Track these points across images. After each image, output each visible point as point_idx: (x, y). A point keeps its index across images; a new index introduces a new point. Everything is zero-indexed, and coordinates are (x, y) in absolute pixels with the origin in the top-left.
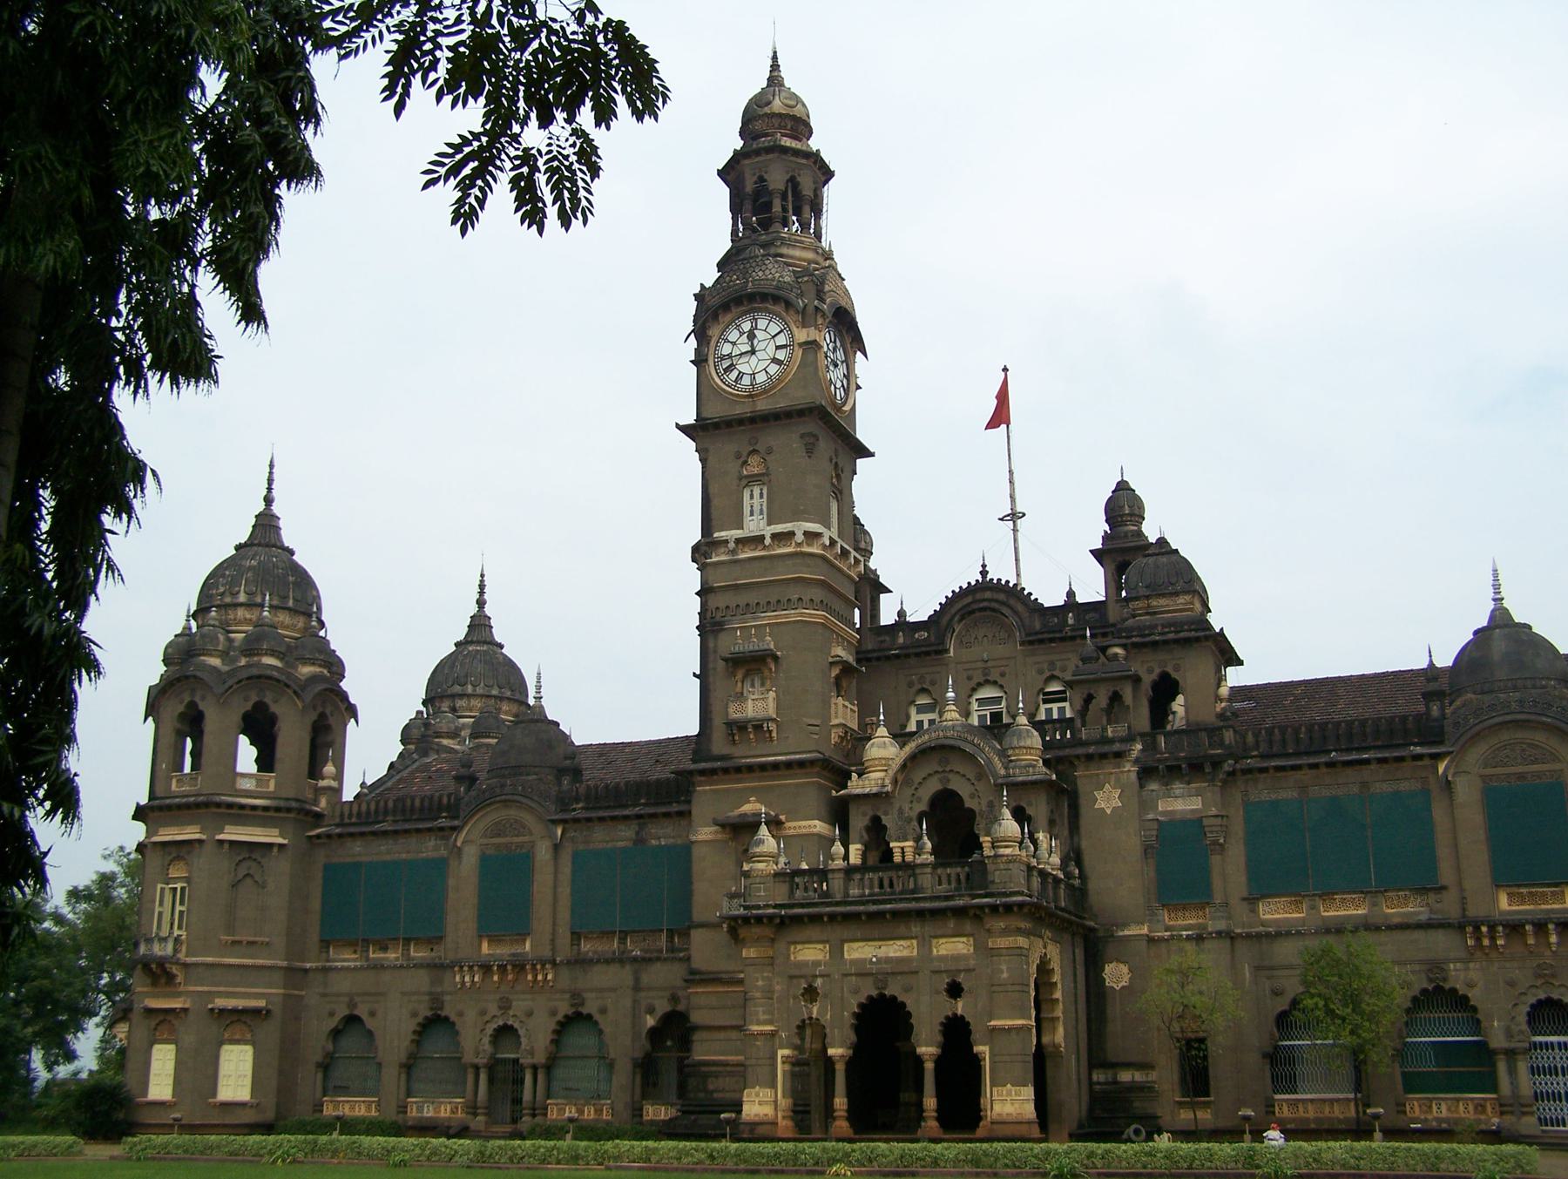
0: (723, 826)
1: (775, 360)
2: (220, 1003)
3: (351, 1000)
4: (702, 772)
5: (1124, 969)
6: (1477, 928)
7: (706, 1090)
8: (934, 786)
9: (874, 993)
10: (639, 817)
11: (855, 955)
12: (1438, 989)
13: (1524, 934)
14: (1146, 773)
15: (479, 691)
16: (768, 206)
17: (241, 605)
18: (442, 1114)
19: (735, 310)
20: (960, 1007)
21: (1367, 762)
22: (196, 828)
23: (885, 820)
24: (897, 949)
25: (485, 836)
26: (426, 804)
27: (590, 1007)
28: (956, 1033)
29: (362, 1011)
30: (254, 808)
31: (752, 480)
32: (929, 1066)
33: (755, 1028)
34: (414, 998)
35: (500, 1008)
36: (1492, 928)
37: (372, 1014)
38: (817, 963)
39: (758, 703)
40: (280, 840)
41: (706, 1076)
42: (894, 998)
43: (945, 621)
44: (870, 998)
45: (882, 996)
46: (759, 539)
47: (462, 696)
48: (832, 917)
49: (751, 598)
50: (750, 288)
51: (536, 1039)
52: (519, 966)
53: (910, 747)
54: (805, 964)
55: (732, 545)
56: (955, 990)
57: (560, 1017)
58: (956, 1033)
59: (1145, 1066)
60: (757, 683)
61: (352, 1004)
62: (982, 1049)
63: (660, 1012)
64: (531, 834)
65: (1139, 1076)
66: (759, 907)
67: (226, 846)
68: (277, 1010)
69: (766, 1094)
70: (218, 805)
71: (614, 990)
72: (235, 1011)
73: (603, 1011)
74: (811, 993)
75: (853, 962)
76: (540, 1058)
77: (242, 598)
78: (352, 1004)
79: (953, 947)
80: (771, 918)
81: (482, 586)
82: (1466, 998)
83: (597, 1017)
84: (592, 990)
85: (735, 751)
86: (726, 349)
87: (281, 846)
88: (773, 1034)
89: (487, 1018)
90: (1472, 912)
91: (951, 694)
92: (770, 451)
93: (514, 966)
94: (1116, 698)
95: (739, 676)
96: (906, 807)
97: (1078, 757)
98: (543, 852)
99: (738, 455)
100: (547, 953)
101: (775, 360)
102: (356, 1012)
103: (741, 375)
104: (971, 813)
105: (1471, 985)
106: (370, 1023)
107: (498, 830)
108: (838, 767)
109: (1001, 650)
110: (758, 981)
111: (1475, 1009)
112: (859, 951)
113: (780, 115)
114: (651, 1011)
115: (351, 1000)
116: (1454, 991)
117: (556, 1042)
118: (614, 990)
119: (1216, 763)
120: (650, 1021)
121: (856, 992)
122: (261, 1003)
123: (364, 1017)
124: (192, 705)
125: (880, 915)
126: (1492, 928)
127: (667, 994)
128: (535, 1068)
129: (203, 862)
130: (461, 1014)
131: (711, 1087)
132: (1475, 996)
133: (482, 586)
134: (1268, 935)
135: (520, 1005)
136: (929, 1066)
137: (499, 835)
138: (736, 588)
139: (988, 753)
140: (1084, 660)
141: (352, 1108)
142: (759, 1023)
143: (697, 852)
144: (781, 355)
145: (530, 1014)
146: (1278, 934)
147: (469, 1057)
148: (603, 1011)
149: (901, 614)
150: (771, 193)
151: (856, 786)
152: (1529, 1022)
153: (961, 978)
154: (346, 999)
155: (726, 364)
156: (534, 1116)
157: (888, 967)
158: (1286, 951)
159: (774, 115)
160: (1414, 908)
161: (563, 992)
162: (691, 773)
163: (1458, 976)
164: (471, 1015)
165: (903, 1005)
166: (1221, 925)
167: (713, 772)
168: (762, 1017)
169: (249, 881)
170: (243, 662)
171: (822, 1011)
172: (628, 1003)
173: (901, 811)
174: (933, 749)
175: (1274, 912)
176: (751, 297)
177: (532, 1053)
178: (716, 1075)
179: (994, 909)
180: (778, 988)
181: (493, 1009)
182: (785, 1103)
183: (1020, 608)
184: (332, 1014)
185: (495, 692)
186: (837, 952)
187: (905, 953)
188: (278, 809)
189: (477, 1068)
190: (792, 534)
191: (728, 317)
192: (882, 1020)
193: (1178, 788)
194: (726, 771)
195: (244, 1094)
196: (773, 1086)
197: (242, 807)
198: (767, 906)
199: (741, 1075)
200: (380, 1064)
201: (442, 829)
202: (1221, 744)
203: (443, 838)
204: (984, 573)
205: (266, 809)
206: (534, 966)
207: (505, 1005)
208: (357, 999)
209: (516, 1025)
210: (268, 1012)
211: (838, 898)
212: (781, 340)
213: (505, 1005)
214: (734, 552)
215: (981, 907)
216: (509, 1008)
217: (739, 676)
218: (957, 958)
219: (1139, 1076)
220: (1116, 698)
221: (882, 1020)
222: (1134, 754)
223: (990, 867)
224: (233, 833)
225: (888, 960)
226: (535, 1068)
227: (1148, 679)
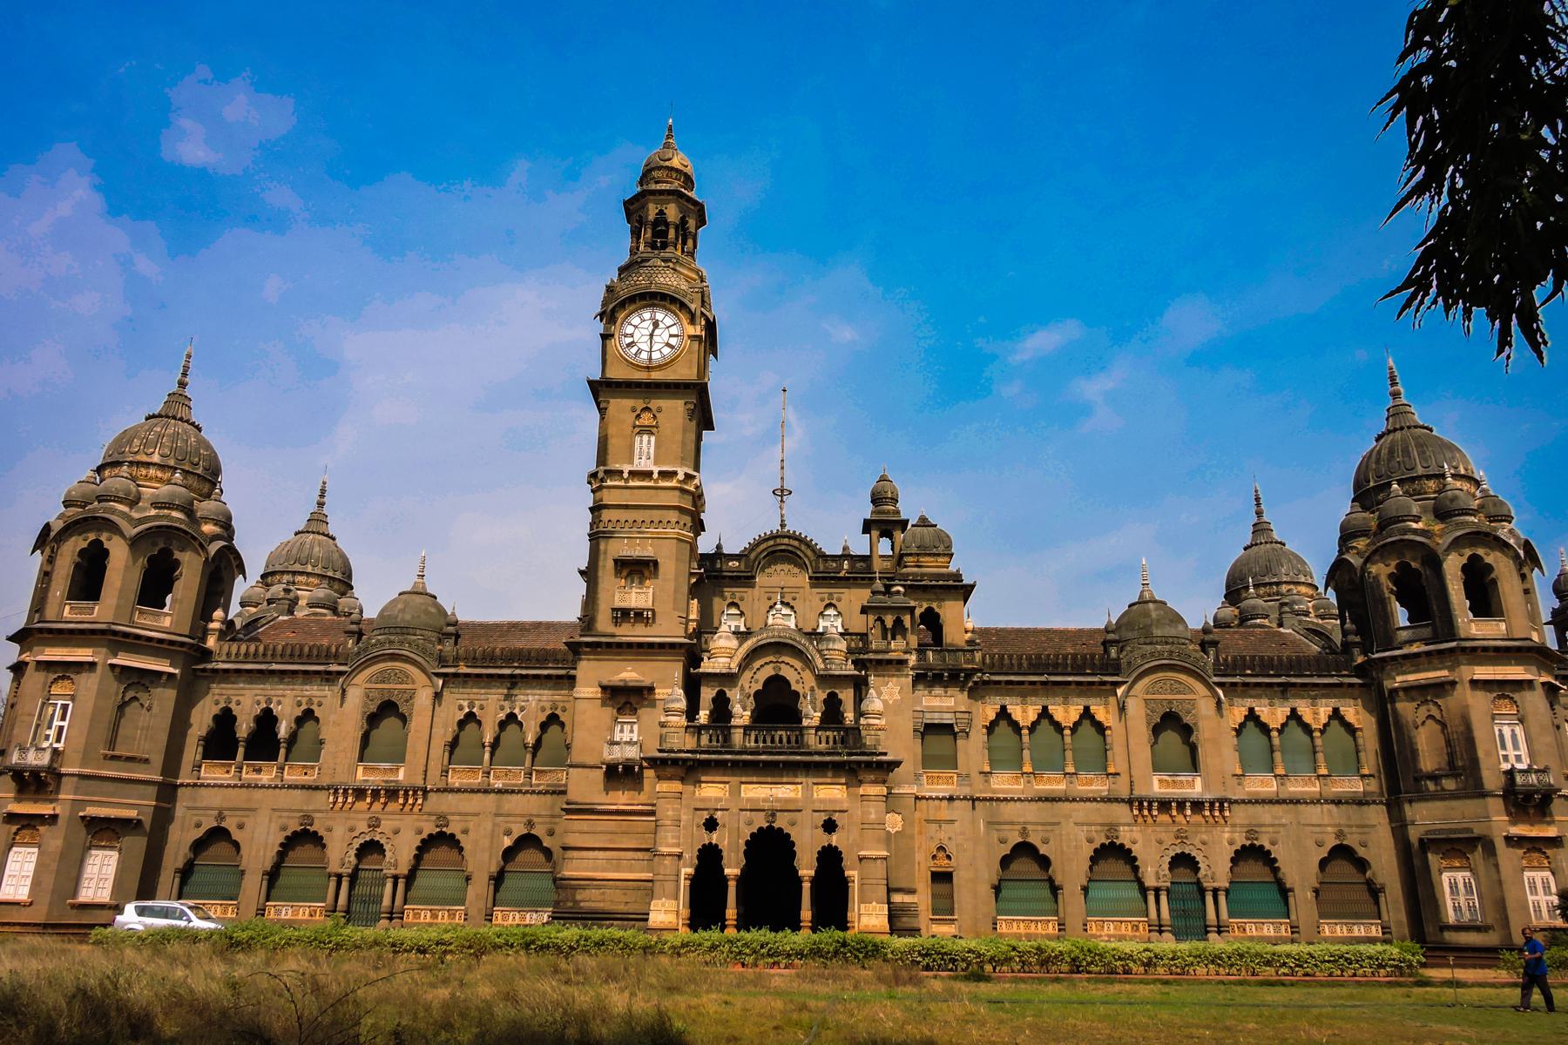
0: (604, 688)
1: (668, 345)
2: (92, 811)
3: (220, 814)
4: (588, 644)
5: (899, 818)
6: (1141, 803)
7: (576, 902)
8: (769, 671)
9: (765, 825)
10: (512, 676)
11: (751, 795)
12: (1112, 843)
13: (1170, 808)
14: (919, 679)
15: (317, 571)
16: (665, 234)
17: (154, 464)
19: (639, 304)
20: (835, 839)
21: (1069, 683)
22: (89, 651)
23: (729, 694)
24: (785, 792)
25: (370, 681)
26: (315, 652)
27: (453, 828)
28: (830, 859)
29: (230, 824)
30: (150, 639)
31: (648, 430)
32: (806, 886)
33: (665, 850)
36: (1150, 803)
37: (241, 827)
38: (720, 800)
39: (637, 597)
40: (171, 670)
41: (575, 888)
42: (780, 830)
43: (752, 556)
44: (761, 829)
45: (770, 828)
46: (649, 475)
47: (301, 573)
48: (735, 764)
49: (639, 515)
50: (653, 290)
51: (400, 853)
52: (392, 793)
53: (750, 643)
54: (709, 799)
55: (626, 475)
56: (830, 826)
57: (424, 835)
58: (830, 859)
59: (912, 892)
60: (636, 581)
61: (221, 817)
62: (852, 873)
63: (516, 835)
65: (907, 899)
66: (671, 751)
67: (117, 670)
68: (147, 821)
69: (670, 904)
70: (115, 633)
71: (477, 815)
72: (107, 820)
74: (711, 825)
75: (748, 800)
76: (404, 869)
77: (156, 458)
78: (221, 817)
79: (832, 793)
80: (685, 760)
81: (323, 491)
82: (1130, 851)
83: (459, 836)
85: (618, 631)
86: (629, 330)
87: (171, 675)
88: (680, 856)
90: (1136, 793)
92: (659, 410)
93: (387, 791)
94: (898, 623)
95: (625, 573)
96: (747, 686)
97: (870, 661)
98: (424, 697)
99: (634, 410)
100: (420, 783)
101: (668, 345)
103: (640, 351)
104: (797, 694)
105: (1134, 843)
106: (236, 835)
107: (383, 677)
108: (692, 654)
109: (792, 581)
110: (667, 811)
111: (1135, 859)
112: (758, 792)
113: (677, 170)
114: (508, 833)
116: (1122, 845)
117: (418, 858)
118: (477, 815)
119: (970, 674)
120: (508, 842)
121: (750, 823)
122: (132, 814)
125: (775, 764)
126: (1150, 803)
128: (396, 878)
129: (88, 684)
130: (330, 830)
131: (578, 897)
132: (1137, 850)
133: (323, 491)
134: (998, 799)
135: (387, 825)
136: (806, 886)
138: (627, 507)
139: (810, 649)
140: (873, 593)
142: (668, 845)
144: (673, 341)
145: (396, 832)
146: (1005, 799)
147: (334, 867)
148: (465, 832)
149: (719, 547)
150: (667, 224)
151: (707, 666)
152: (1170, 869)
153: (836, 817)
155: (629, 340)
156: (391, 919)
157: (778, 806)
158: (1008, 810)
159: (672, 169)
160: (1100, 787)
161: (430, 814)
162: (580, 644)
163: (1125, 836)
165: (788, 836)
166: (966, 791)
167: (598, 644)
168: (671, 841)
169: (136, 704)
170: (153, 512)
171: (720, 838)
172: (489, 826)
173: (742, 689)
174: (769, 644)
175: (1003, 783)
176: (653, 295)
177: (396, 866)
178: (584, 888)
179: (869, 765)
180: (684, 817)
181: (362, 826)
182: (685, 912)
183: (809, 553)
184: (198, 825)
185: (330, 574)
186: (735, 792)
187: (792, 795)
188: (172, 643)
189: (339, 877)
190: (675, 473)
191: (632, 307)
192: (770, 846)
193: (938, 691)
194: (609, 645)
195: (23, 894)
196: (677, 898)
197: (138, 637)
198: (680, 751)
199: (648, 889)
200: (243, 873)
201: (329, 673)
202: (973, 661)
204: (783, 526)
205: (161, 641)
206: (406, 792)
207: (374, 824)
210: (139, 821)
211: (737, 748)
212: (674, 330)
213: (374, 824)
214: (627, 480)
215: (859, 763)
217: (625, 573)
218: (831, 801)
219: (907, 899)
220: (898, 623)
221: (770, 846)
222: (911, 664)
223: (863, 733)
224: (123, 660)
225: (778, 800)
226: (396, 878)
227: (918, 612)
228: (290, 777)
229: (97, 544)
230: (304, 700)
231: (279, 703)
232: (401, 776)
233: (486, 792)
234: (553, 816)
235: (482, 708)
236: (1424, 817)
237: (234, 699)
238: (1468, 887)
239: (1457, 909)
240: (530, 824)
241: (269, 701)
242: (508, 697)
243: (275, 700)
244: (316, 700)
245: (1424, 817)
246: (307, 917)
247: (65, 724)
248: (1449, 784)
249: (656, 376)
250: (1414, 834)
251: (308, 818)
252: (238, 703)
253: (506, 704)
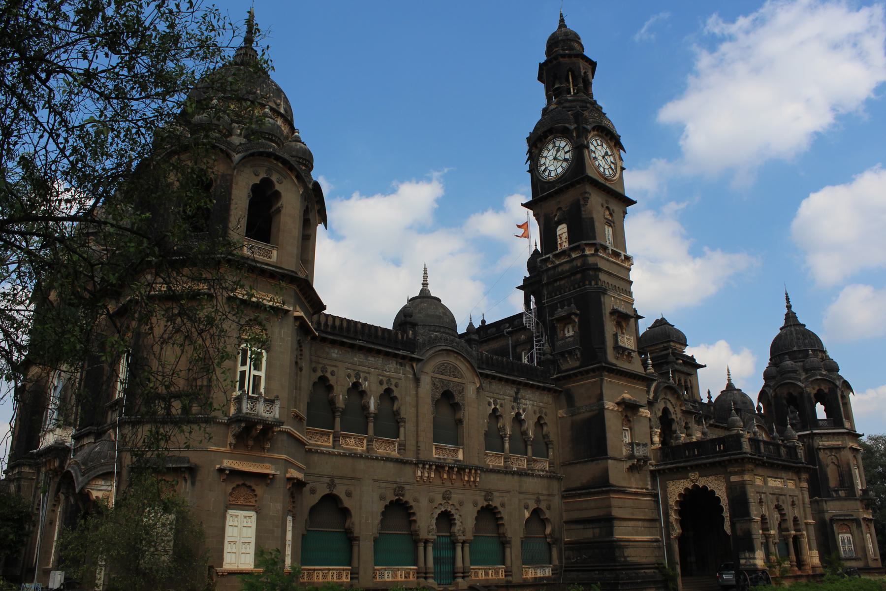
3: (332, 481)
7: (625, 557)
10: (520, 383)
18: (399, 579)
27: (496, 502)
34: (383, 485)
35: (444, 498)
61: (332, 485)
64: (462, 377)
71: (508, 492)
73: (503, 505)
78: (332, 485)
84: (498, 491)
89: (435, 504)
91: (650, 362)
102: (335, 492)
114: (526, 507)
115: (332, 481)
118: (508, 492)
123: (342, 496)
124: (266, 183)
127: (535, 497)
135: (456, 497)
137: (443, 374)
141: (324, 576)
143: (607, 415)
154: (327, 480)
164: (424, 503)
177: (464, 533)
181: (439, 499)
203: (401, 365)
207: (446, 497)
208: (336, 481)
209: (453, 512)
213: (446, 497)
216: (449, 499)
228: (381, 450)
229: (266, 183)
230: (385, 379)
231: (366, 379)
232: (460, 456)
233: (506, 473)
234: (549, 495)
235: (501, 406)
236: (832, 508)
237: (330, 369)
238: (849, 540)
239: (845, 551)
240: (538, 501)
241: (358, 376)
242: (516, 399)
243: (362, 375)
244: (393, 381)
245: (832, 508)
246: (403, 579)
247: (262, 374)
248: (842, 493)
249: (608, 184)
250: (827, 517)
251: (400, 490)
252: (332, 374)
253: (515, 404)
